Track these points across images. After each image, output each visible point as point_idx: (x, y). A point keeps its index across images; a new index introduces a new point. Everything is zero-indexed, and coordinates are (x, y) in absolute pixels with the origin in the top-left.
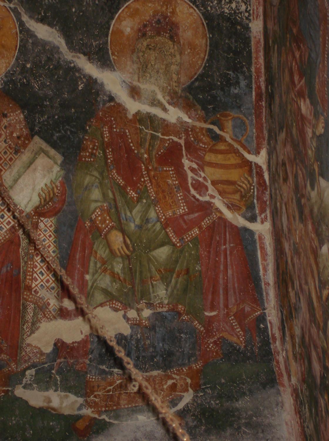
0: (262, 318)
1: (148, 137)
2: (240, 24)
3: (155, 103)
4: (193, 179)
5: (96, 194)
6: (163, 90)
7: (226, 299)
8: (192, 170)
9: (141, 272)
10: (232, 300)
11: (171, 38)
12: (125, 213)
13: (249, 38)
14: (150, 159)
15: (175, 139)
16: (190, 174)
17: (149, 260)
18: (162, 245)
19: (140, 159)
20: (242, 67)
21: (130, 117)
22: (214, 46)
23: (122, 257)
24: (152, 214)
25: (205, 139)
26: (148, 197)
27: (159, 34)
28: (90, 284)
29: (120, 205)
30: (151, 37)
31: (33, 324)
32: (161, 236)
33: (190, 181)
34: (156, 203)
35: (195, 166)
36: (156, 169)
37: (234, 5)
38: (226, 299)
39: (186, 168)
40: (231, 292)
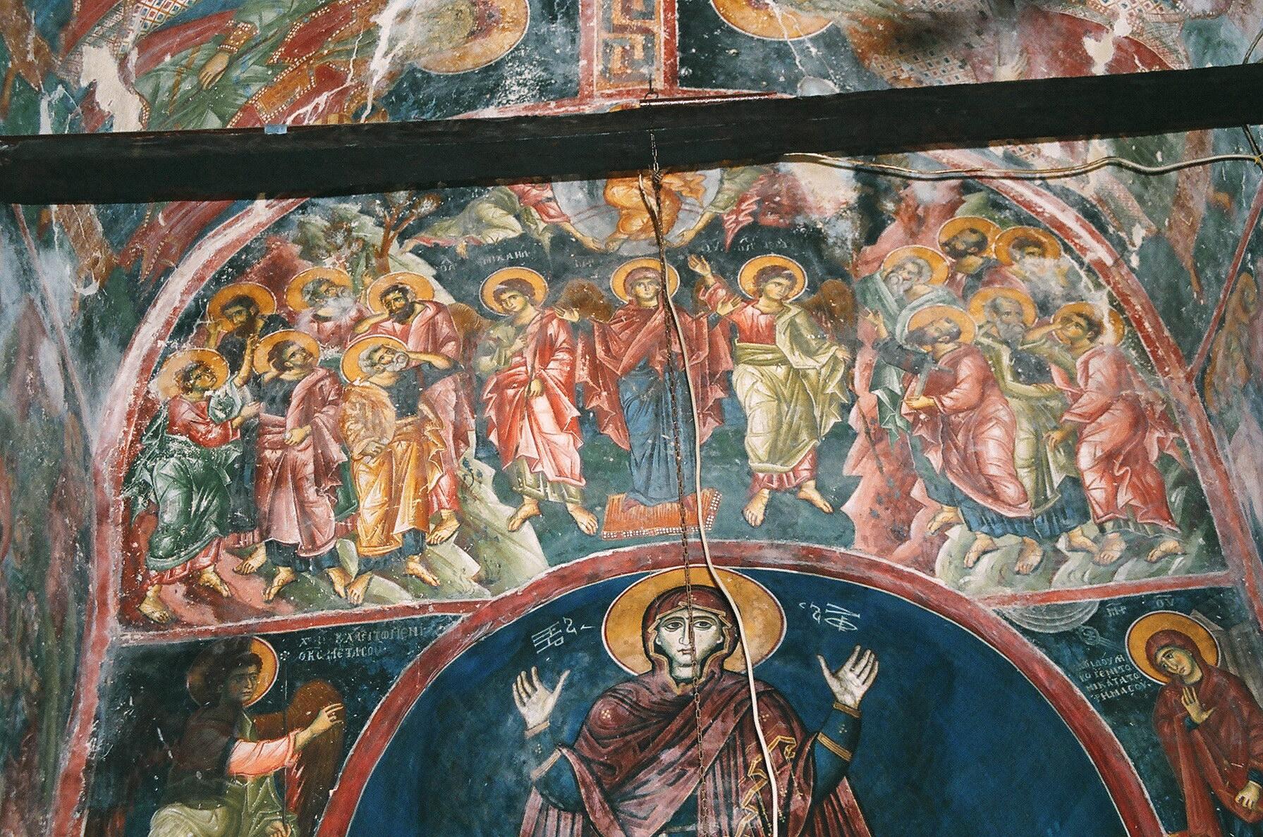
0: (168, 271)
1: (349, 47)
2: (491, 98)
3: (393, 42)
4: (305, 114)
5: (269, 16)
6: (410, 44)
7: (178, 222)
8: (316, 108)
9: (186, 115)
10: (179, 228)
11: (472, 33)
12: (250, 59)
13: (476, 108)
14: (322, 57)
15: (350, 76)
16: (309, 108)
17: (201, 114)
18: (221, 117)
19: (322, 47)
20: (441, 110)
21: (372, 20)
22: (464, 78)
23: (199, 82)
24: (254, 88)
25: (354, 106)
26: (275, 74)
27: (476, 19)
28: (161, 66)
29: (261, 47)
30: (471, 13)
31: (102, 37)
32: (231, 110)
33: (302, 111)
34: (270, 85)
35: (320, 109)
36: (310, 68)
37: (516, 88)
38: (178, 222)
39: (317, 100)
40: (185, 220)
